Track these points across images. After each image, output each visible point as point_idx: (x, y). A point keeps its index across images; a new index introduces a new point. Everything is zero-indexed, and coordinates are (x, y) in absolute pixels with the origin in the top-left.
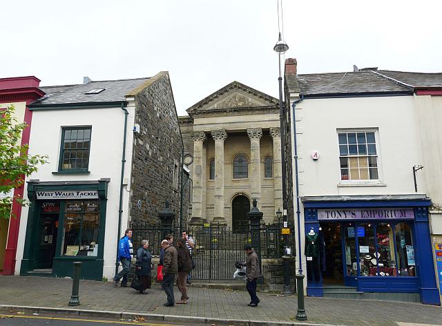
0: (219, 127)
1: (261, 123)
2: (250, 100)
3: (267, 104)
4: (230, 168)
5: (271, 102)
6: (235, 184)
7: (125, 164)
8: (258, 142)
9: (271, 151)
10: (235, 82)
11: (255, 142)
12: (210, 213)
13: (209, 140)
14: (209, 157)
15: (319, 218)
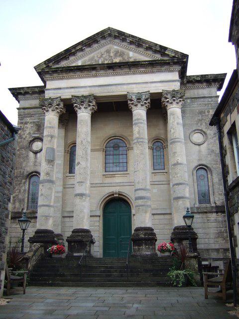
1: (149, 85)
3: (158, 57)
4: (100, 156)
6: (108, 180)
9: (162, 132)
10: (109, 28)
11: (140, 113)
12: (68, 224)
13: (68, 115)
14: (69, 141)
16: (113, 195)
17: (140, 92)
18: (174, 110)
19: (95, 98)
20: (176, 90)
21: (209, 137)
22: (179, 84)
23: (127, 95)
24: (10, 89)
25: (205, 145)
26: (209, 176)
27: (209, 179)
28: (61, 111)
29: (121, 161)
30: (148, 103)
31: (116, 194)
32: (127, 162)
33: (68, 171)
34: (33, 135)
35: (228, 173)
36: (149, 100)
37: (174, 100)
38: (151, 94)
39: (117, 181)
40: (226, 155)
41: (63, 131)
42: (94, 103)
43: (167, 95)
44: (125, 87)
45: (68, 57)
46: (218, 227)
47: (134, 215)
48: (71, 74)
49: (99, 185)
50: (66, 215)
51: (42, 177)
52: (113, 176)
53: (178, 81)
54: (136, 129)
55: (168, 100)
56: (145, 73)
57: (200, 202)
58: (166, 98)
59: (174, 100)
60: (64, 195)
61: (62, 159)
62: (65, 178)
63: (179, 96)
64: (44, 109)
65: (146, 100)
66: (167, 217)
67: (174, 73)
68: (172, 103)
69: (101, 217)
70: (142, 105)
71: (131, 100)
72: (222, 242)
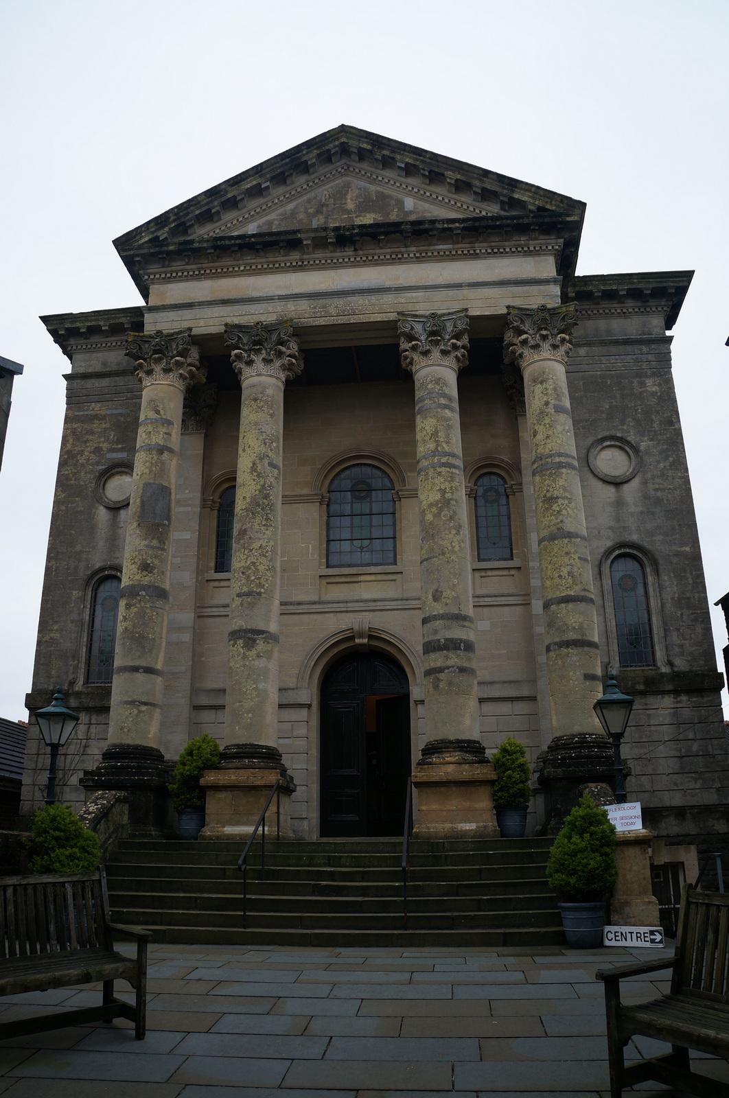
0: (266, 314)
2: (409, 203)
3: (491, 209)
4: (311, 514)
5: (513, 203)
6: (337, 592)
8: (451, 377)
14: (218, 473)
16: (352, 638)
17: (439, 312)
19: (300, 332)
20: (549, 306)
22: (556, 290)
23: (396, 321)
24: (45, 319)
25: (635, 483)
26: (650, 579)
27: (651, 589)
28: (190, 372)
29: (376, 533)
30: (464, 347)
31: (361, 635)
32: (394, 538)
33: (212, 564)
34: (110, 456)
36: (465, 340)
38: (473, 318)
39: (366, 596)
41: (196, 444)
42: (294, 347)
43: (522, 322)
44: (388, 298)
45: (218, 213)
46: (681, 737)
47: (422, 702)
48: (227, 262)
49: (305, 608)
50: (204, 700)
51: (129, 576)
52: (352, 579)
53: (555, 281)
54: (425, 425)
57: (624, 662)
58: (521, 332)
59: (544, 338)
60: (199, 636)
61: (195, 525)
62: (202, 584)
63: (560, 325)
64: (141, 366)
65: (457, 336)
66: (521, 708)
67: (543, 258)
69: (315, 708)
70: (445, 353)
71: (411, 338)
72: (692, 785)
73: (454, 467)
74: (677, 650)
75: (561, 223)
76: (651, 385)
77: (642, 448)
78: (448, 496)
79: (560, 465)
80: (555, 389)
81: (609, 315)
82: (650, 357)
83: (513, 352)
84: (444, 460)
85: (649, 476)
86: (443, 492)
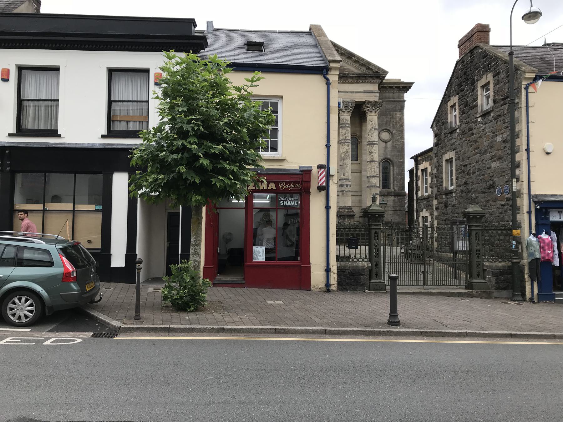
1: (354, 94)
3: (363, 70)
5: (368, 68)
7: (331, 148)
15: (551, 219)
18: (373, 118)
21: (395, 136)
22: (378, 95)
25: (391, 142)
35: (419, 190)
37: (373, 109)
40: (419, 180)
46: (395, 206)
53: (378, 92)
55: (369, 108)
56: (352, 83)
58: (368, 107)
59: (373, 109)
66: (358, 197)
68: (371, 112)
70: (348, 112)
72: (396, 217)
73: (349, 143)
74: (396, 185)
75: (382, 77)
76: (398, 115)
77: (394, 133)
78: (347, 151)
79: (374, 144)
80: (375, 124)
81: (389, 92)
82: (399, 106)
83: (365, 111)
84: (347, 141)
85: (394, 140)
86: (346, 149)
